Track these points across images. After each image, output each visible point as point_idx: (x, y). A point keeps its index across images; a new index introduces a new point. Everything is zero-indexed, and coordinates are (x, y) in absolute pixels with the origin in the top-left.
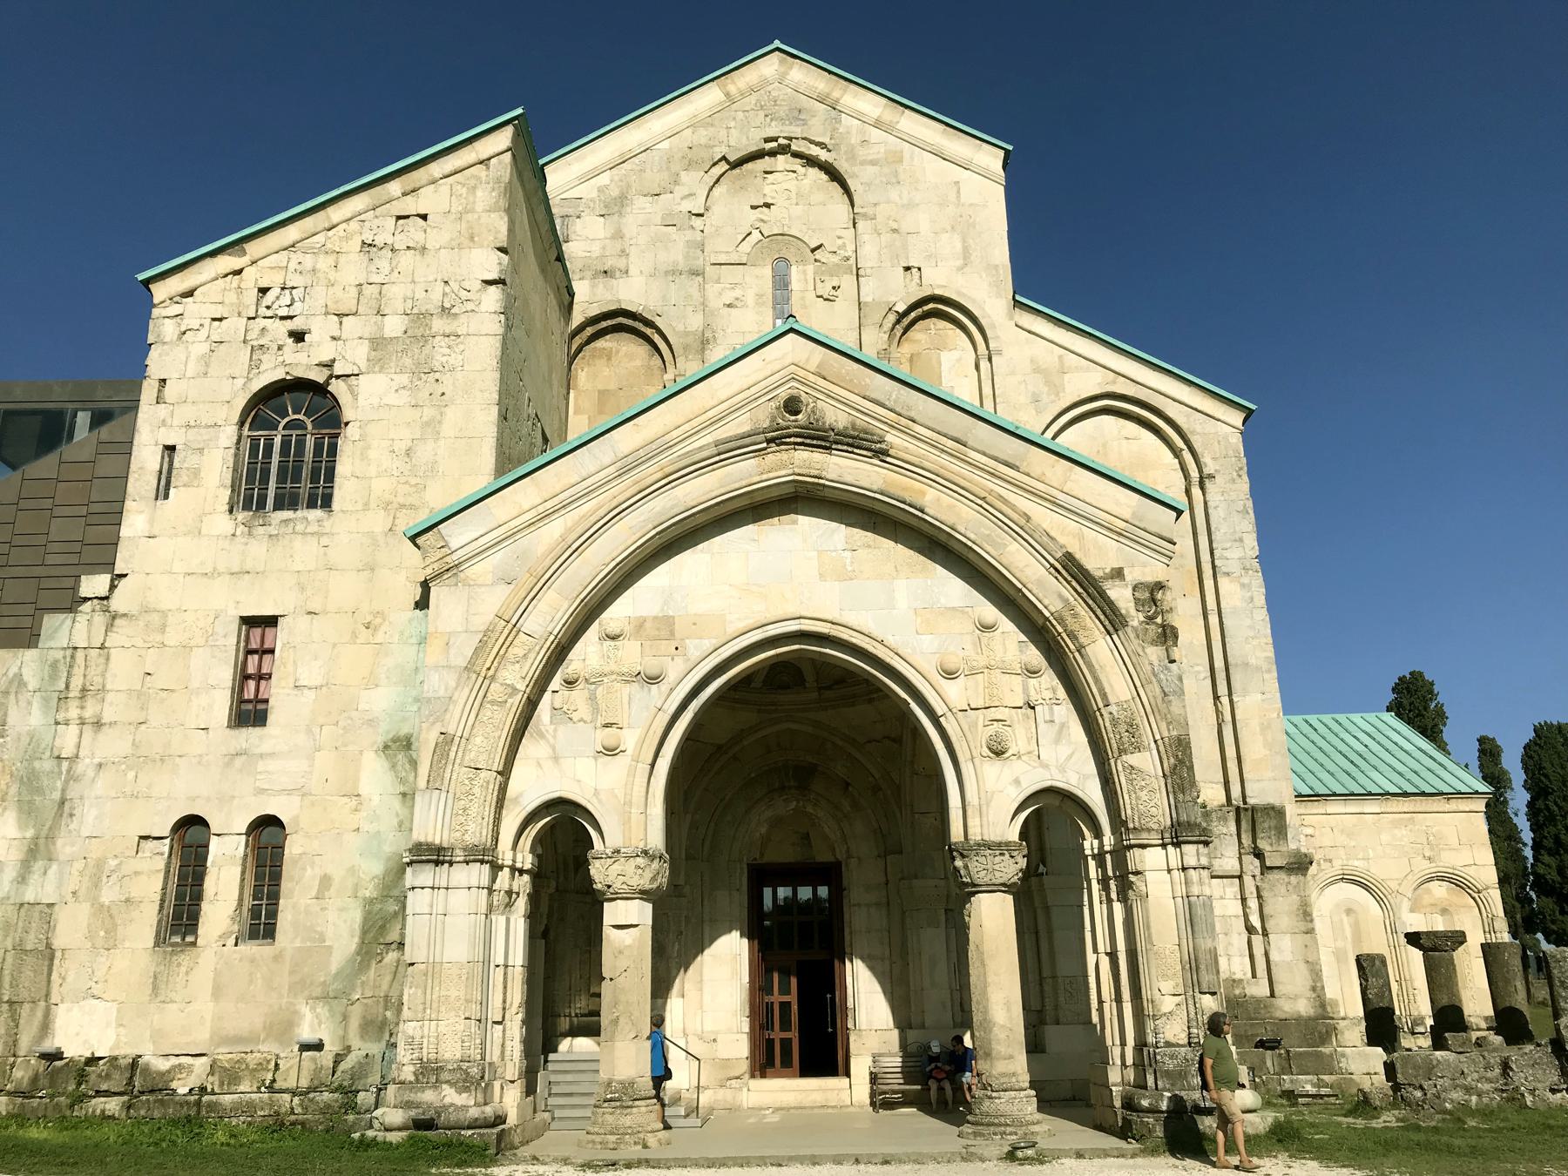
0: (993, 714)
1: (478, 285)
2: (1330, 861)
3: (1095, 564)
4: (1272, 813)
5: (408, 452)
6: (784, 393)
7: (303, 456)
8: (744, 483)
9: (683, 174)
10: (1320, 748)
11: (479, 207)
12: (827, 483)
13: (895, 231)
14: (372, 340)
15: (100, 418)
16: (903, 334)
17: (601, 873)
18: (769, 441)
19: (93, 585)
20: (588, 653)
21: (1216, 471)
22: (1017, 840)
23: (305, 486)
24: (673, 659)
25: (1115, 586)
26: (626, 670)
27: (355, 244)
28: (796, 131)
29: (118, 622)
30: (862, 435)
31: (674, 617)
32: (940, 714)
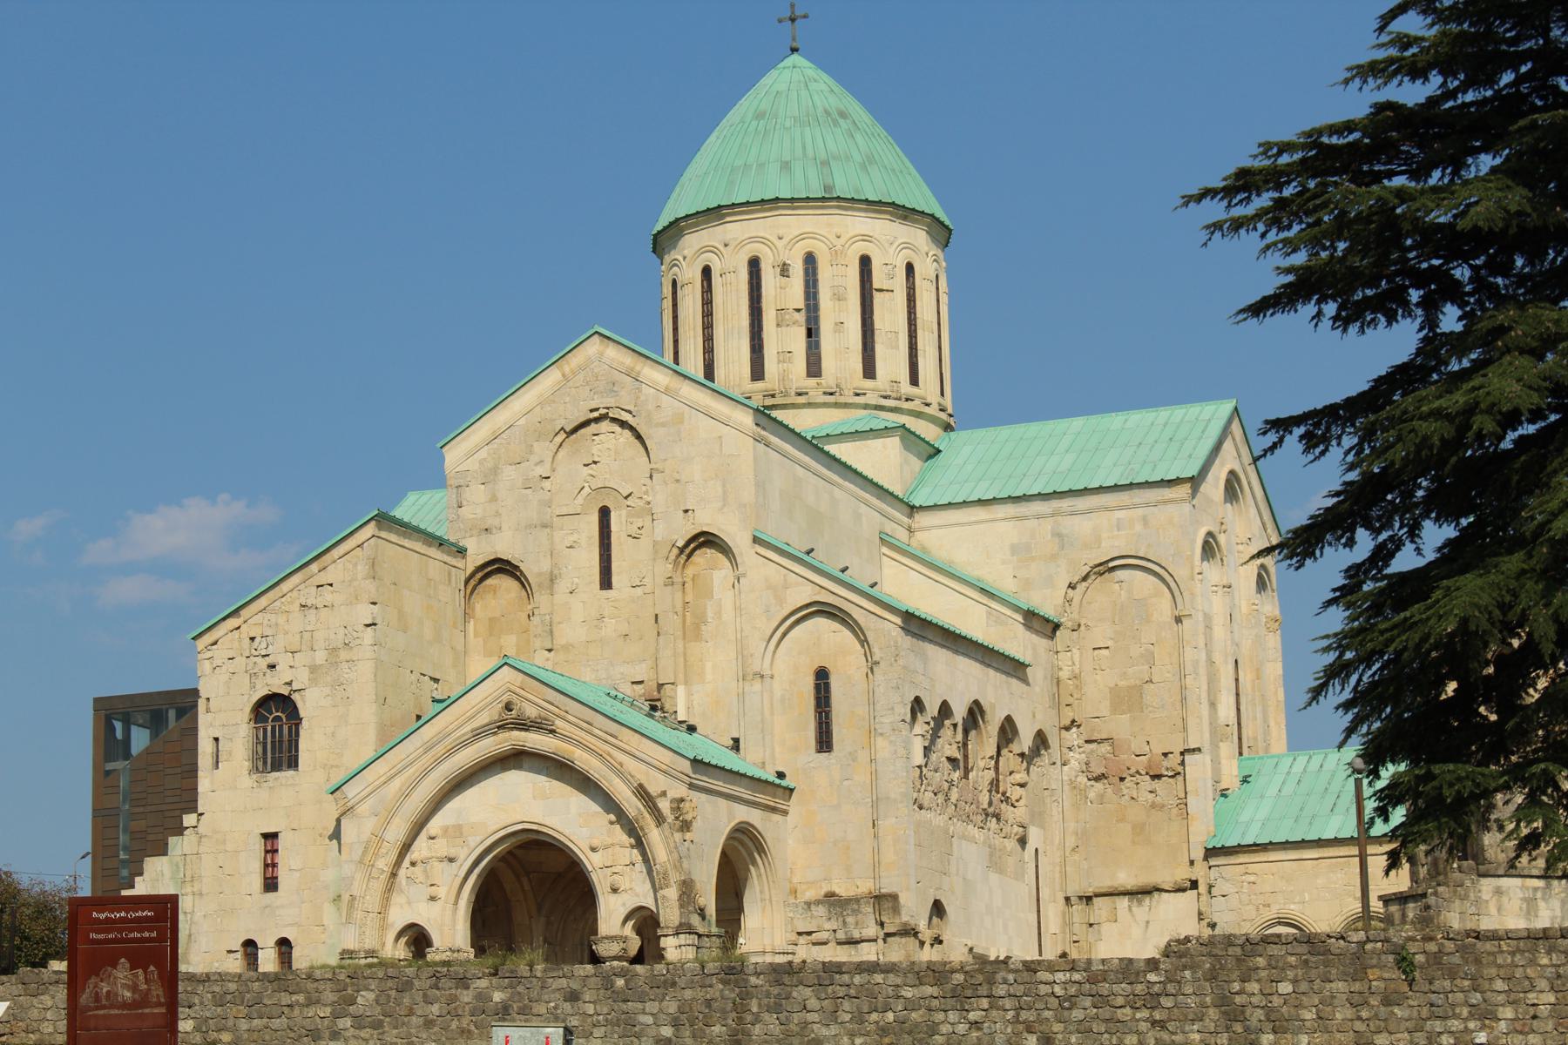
0: (614, 869)
1: (361, 628)
3: (653, 790)
5: (333, 734)
9: (535, 444)
11: (360, 577)
13: (678, 481)
14: (310, 667)
15: (181, 713)
16: (687, 560)
19: (189, 820)
20: (421, 848)
21: (881, 658)
23: (285, 756)
27: (296, 606)
28: (611, 402)
29: (203, 840)
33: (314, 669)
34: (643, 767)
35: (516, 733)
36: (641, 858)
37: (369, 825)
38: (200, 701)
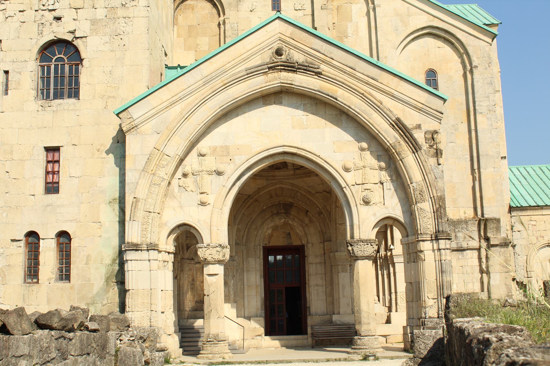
0: (366, 186)
2: (543, 237)
3: (409, 123)
4: (495, 221)
5: (111, 73)
6: (276, 46)
7: (65, 74)
8: (258, 87)
10: (544, 182)
12: (295, 87)
17: (201, 253)
18: (269, 68)
21: (478, 64)
22: (374, 238)
23: (66, 88)
24: (229, 164)
25: (417, 132)
26: (209, 170)
30: (310, 65)
31: (229, 146)
32: (343, 186)
33: (94, 22)
34: (400, 106)
35: (284, 74)
36: (389, 178)
37: (152, 141)
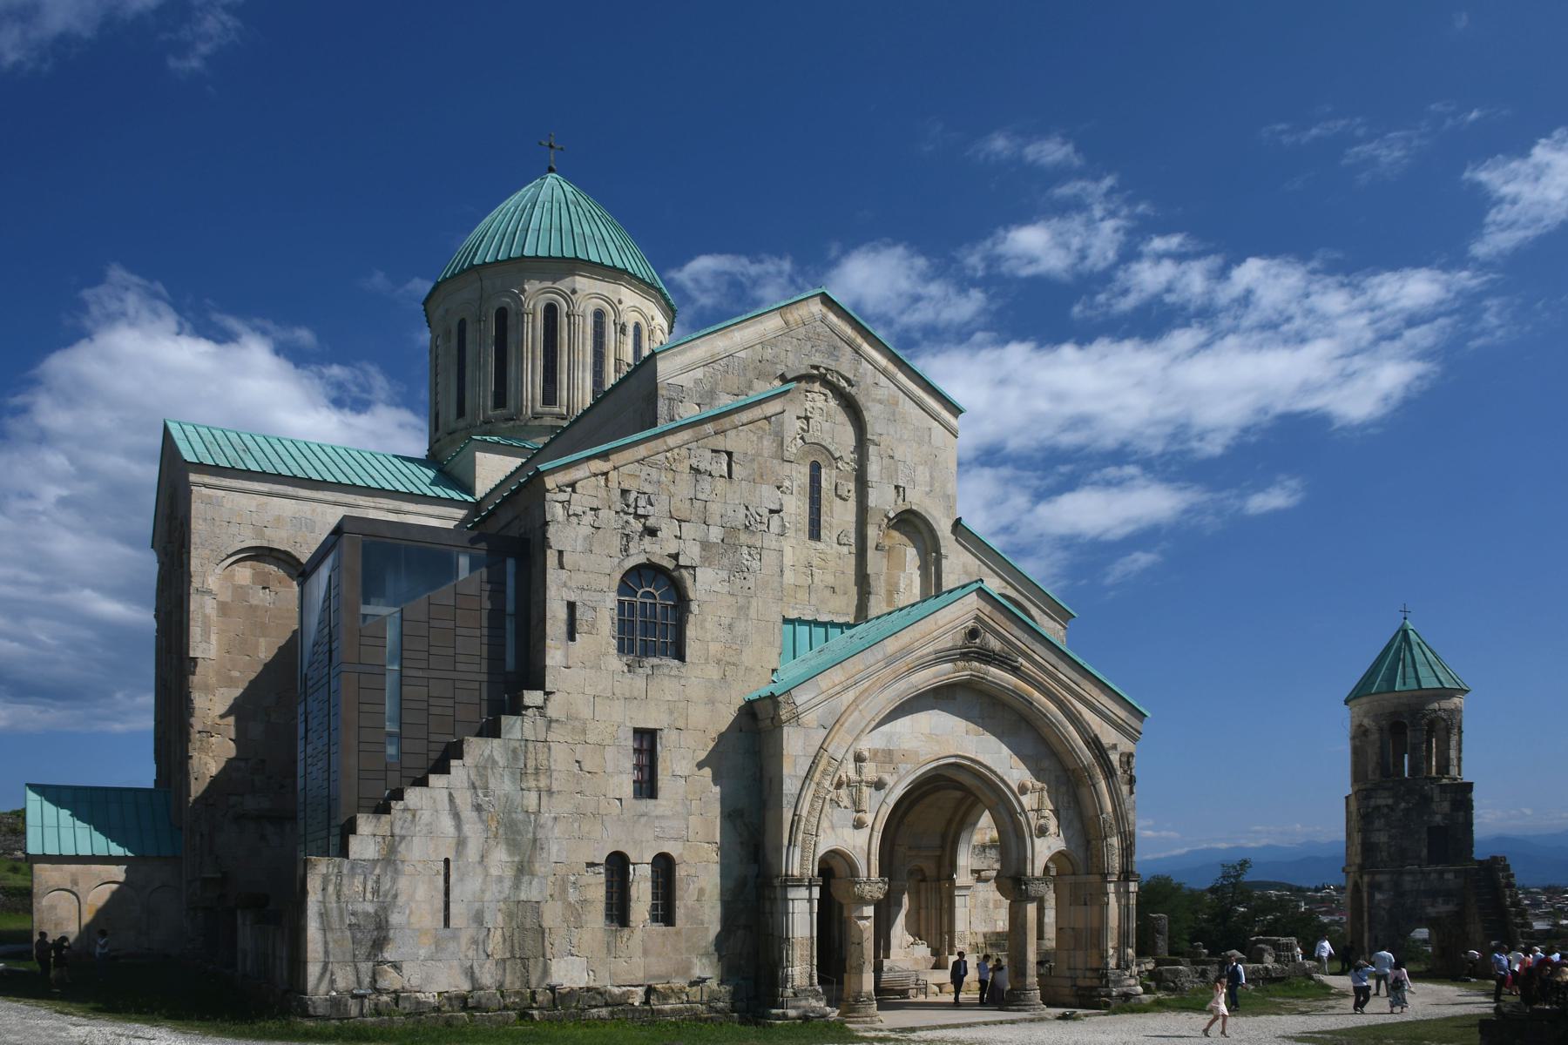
5: (730, 627)
33: (705, 545)
38: (549, 552)
